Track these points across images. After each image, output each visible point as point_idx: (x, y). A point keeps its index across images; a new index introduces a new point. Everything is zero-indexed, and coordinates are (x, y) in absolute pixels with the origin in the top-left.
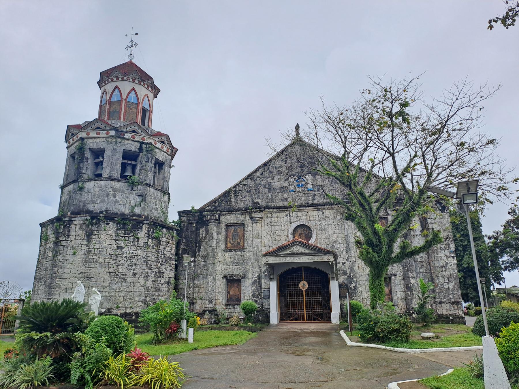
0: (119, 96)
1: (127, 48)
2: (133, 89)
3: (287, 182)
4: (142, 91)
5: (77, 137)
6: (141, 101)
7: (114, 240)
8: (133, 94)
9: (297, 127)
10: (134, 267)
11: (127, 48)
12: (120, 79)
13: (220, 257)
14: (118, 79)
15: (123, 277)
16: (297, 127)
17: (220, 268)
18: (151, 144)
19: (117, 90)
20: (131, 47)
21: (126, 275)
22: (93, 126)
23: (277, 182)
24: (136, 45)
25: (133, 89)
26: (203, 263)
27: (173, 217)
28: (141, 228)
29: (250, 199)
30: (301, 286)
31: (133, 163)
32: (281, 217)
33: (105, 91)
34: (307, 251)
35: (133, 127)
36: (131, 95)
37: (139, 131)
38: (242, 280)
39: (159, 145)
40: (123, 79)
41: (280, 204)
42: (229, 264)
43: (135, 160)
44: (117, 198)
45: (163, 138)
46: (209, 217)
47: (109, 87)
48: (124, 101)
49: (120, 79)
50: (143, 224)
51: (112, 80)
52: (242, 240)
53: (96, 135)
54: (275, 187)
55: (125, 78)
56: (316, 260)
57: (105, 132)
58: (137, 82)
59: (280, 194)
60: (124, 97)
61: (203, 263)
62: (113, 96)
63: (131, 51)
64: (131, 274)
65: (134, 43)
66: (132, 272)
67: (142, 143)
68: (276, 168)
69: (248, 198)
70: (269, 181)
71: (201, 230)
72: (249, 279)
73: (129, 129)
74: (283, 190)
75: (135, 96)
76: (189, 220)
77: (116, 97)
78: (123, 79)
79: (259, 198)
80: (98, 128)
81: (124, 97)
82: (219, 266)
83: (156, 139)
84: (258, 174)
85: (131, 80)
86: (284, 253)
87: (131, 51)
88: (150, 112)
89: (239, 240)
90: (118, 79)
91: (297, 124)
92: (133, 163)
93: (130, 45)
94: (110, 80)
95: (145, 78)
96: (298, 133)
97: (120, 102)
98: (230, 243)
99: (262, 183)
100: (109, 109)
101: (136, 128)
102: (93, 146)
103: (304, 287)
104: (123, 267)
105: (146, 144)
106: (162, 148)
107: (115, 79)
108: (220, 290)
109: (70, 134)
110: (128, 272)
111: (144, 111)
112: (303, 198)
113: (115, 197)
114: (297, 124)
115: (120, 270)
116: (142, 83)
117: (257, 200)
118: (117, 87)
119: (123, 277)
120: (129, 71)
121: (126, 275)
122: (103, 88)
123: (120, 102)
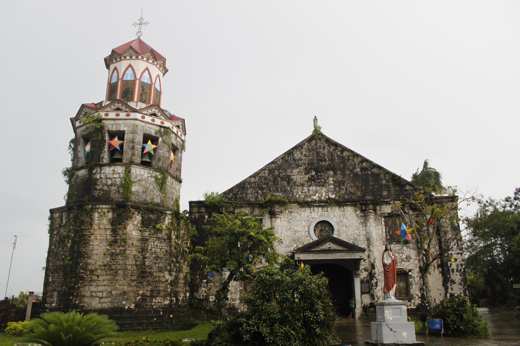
0: (133, 75)
1: (135, 24)
2: (147, 69)
4: (155, 71)
7: (140, 231)
8: (146, 74)
9: (315, 119)
10: (159, 261)
11: (135, 24)
14: (131, 57)
15: (149, 270)
16: (315, 119)
18: (169, 128)
19: (130, 69)
20: (140, 24)
21: (152, 268)
22: (113, 107)
25: (147, 69)
27: (184, 207)
32: (306, 212)
33: (116, 68)
34: (340, 248)
35: (154, 110)
36: (144, 74)
37: (159, 114)
39: (175, 130)
45: (179, 122)
47: (122, 65)
48: (138, 81)
51: (125, 57)
53: (115, 117)
56: (348, 257)
58: (150, 61)
62: (125, 75)
64: (157, 268)
65: (144, 21)
66: (157, 265)
67: (161, 126)
73: (150, 111)
75: (148, 76)
77: (129, 77)
78: (137, 57)
80: (118, 109)
81: (138, 77)
83: (173, 123)
85: (145, 59)
86: (317, 249)
88: (160, 93)
90: (131, 57)
91: (315, 117)
93: (138, 22)
94: (123, 58)
95: (156, 57)
97: (134, 82)
102: (112, 128)
104: (149, 260)
107: (128, 58)
109: (83, 113)
110: (154, 265)
114: (315, 117)
115: (147, 263)
116: (156, 63)
118: (130, 66)
119: (149, 270)
120: (138, 49)
121: (152, 268)
122: (112, 67)
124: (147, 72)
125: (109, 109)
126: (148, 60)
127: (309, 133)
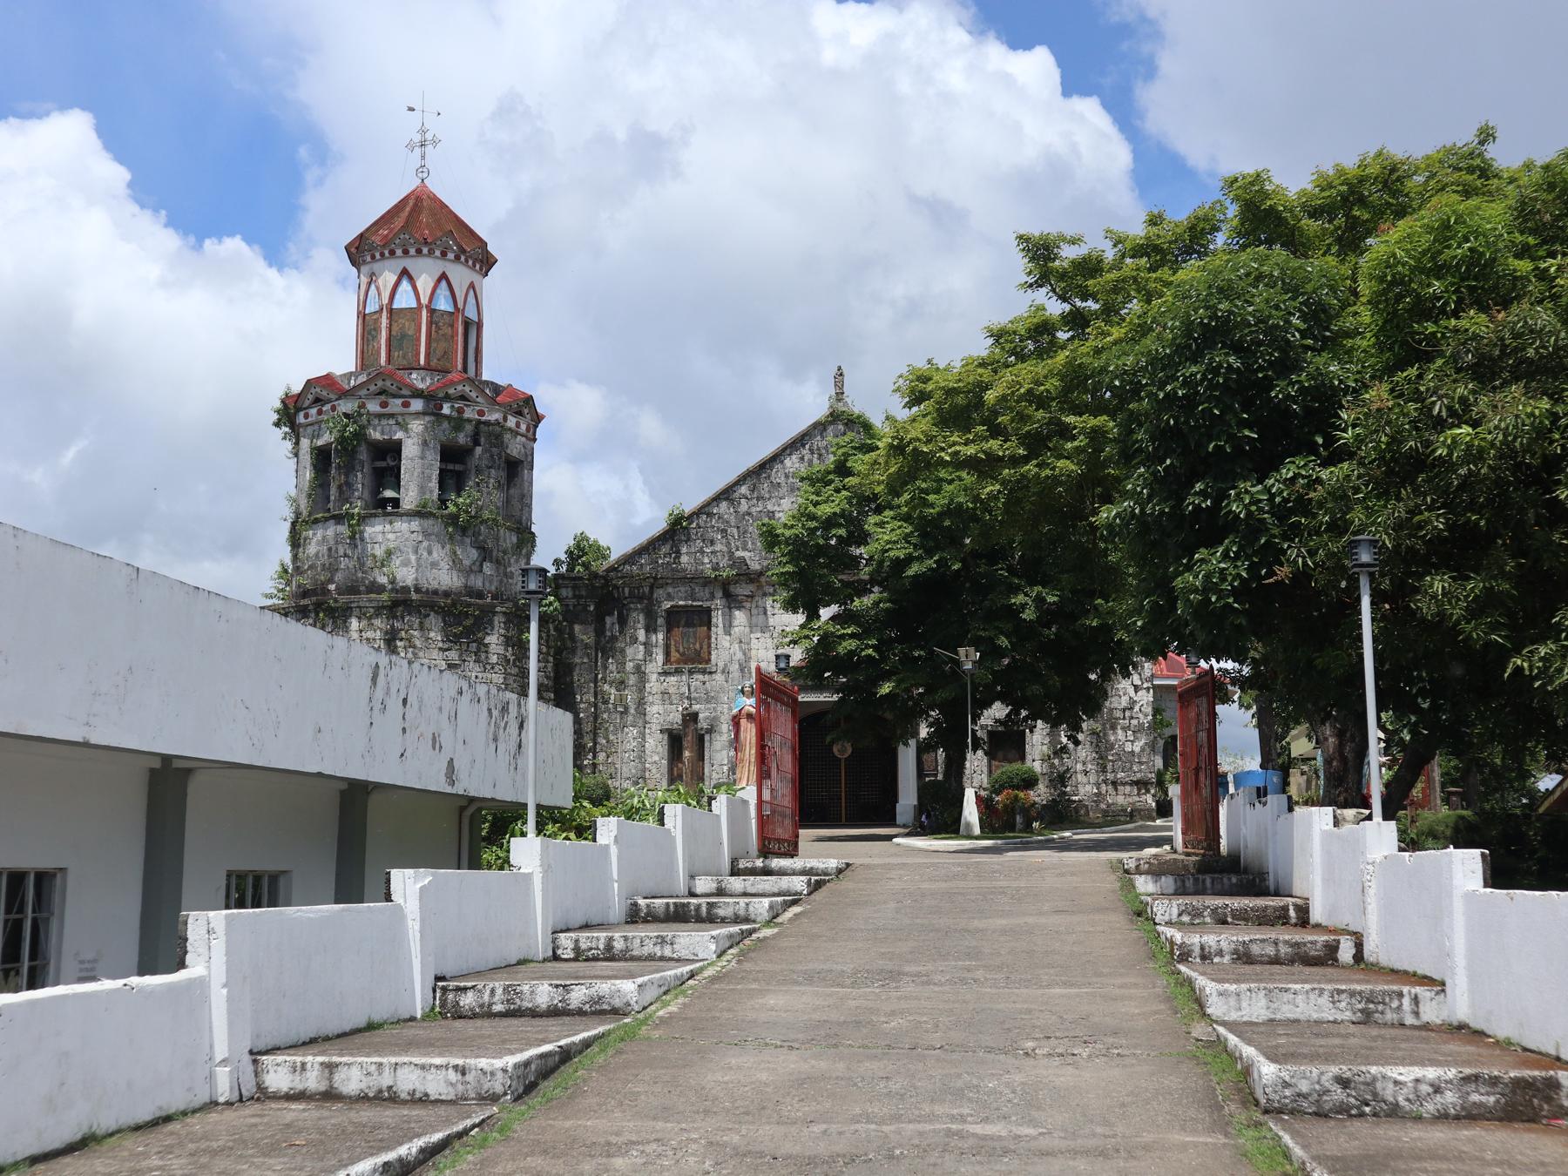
5: (334, 408)
6: (460, 305)
8: (443, 288)
11: (410, 146)
12: (412, 251)
13: (654, 684)
14: (406, 252)
17: (655, 709)
24: (435, 142)
28: (491, 623)
31: (458, 467)
37: (473, 395)
38: (707, 737)
39: (511, 422)
40: (419, 251)
42: (675, 699)
43: (463, 462)
44: (435, 555)
49: (412, 251)
50: (495, 613)
51: (392, 253)
55: (425, 250)
57: (399, 401)
58: (451, 256)
60: (424, 301)
63: (423, 157)
67: (479, 422)
68: (787, 476)
69: (718, 547)
70: (770, 507)
71: (608, 620)
72: (721, 733)
76: (580, 597)
78: (419, 251)
79: (745, 549)
81: (424, 301)
82: (652, 703)
84: (744, 490)
87: (423, 157)
88: (479, 325)
90: (406, 252)
92: (458, 467)
93: (417, 138)
96: (840, 395)
99: (753, 510)
100: (390, 329)
101: (467, 389)
103: (842, 751)
105: (487, 423)
106: (518, 425)
107: (399, 252)
108: (656, 758)
111: (467, 324)
113: (430, 553)
117: (739, 554)
123: (414, 313)
124: (444, 283)
125: (363, 392)
126: (444, 254)
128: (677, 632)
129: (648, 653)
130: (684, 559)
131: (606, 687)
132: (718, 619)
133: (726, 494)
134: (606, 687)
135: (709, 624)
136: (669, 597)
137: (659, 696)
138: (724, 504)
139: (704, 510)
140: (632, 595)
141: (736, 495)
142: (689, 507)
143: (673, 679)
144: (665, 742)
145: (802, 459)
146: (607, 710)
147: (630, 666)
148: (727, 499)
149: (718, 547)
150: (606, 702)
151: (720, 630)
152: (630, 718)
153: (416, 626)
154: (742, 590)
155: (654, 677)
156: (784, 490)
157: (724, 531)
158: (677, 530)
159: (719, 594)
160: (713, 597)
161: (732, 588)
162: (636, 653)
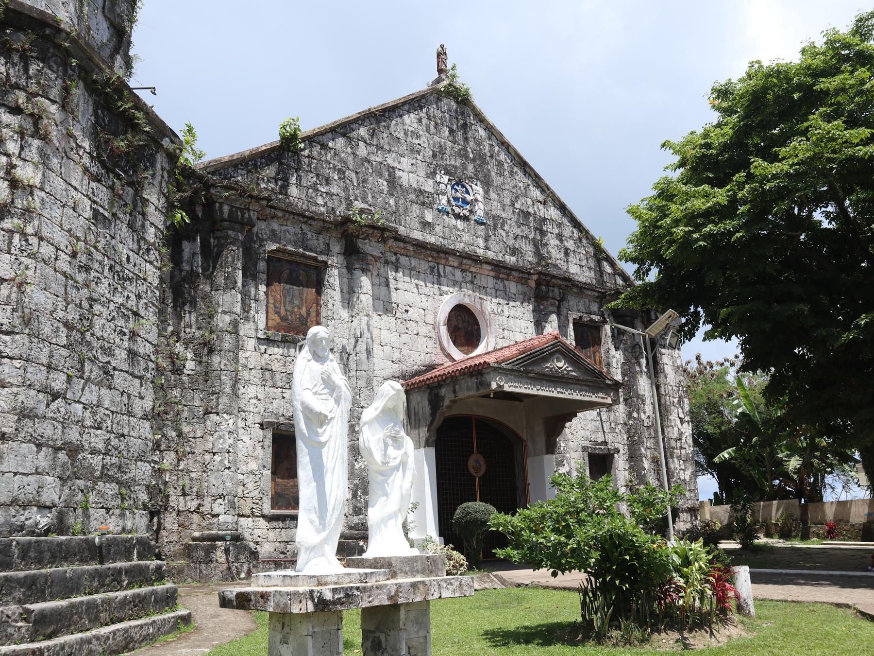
3: (430, 182)
9: (441, 55)
16: (441, 55)
23: (411, 173)
26: (190, 365)
29: (342, 194)
30: (471, 463)
41: (417, 235)
46: (226, 209)
52: (313, 314)
54: (405, 183)
59: (415, 209)
61: (190, 365)
68: (406, 133)
70: (390, 161)
71: (187, 247)
74: (424, 199)
82: (248, 382)
84: (363, 131)
89: (304, 311)
98: (278, 313)
99: (373, 158)
103: (477, 469)
108: (253, 466)
112: (466, 238)
127: (421, 80)
128: (277, 287)
129: (246, 308)
130: (293, 191)
131: (179, 348)
132: (334, 277)
133: (343, 129)
134: (179, 348)
135: (319, 285)
136: (274, 237)
137: (257, 373)
138: (340, 143)
139: (315, 139)
140: (232, 219)
141: (354, 134)
142: (306, 128)
143: (277, 351)
144: (268, 442)
145: (420, 120)
146: (180, 384)
147: (222, 321)
148: (344, 135)
149: (335, 189)
150: (177, 371)
151: (337, 295)
152: (224, 400)
153: (55, 93)
154: (371, 247)
155: (251, 344)
156: (403, 148)
157: (341, 172)
158: (286, 152)
159: (336, 248)
160: (327, 252)
161: (360, 243)
162: (229, 301)
